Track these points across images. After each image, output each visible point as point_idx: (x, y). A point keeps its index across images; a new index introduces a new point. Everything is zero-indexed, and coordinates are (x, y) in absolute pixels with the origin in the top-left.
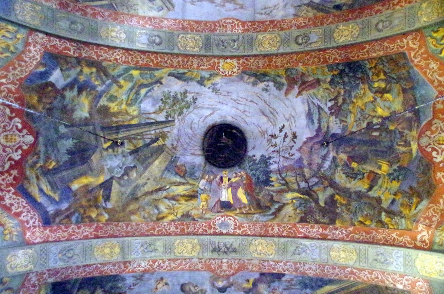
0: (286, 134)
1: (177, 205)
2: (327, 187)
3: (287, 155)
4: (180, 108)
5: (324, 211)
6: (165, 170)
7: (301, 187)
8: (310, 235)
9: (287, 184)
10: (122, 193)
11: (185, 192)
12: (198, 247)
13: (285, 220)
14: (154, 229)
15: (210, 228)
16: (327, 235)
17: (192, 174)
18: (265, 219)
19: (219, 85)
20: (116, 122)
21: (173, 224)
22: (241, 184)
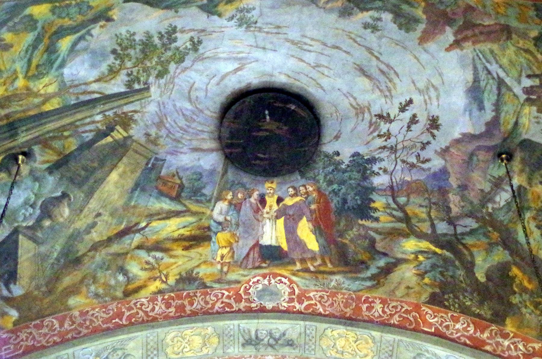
0: (414, 116)
1: (167, 260)
2: (497, 244)
3: (413, 160)
4: (160, 63)
5: (483, 293)
6: (133, 190)
7: (439, 232)
8: (448, 333)
9: (407, 219)
10: (44, 258)
11: (182, 231)
12: (215, 340)
13: (399, 293)
14: (120, 315)
15: (239, 299)
16: (484, 343)
17: (196, 193)
18: (356, 285)
19: (255, 13)
20: (7, 116)
21: (160, 299)
22: (306, 210)
